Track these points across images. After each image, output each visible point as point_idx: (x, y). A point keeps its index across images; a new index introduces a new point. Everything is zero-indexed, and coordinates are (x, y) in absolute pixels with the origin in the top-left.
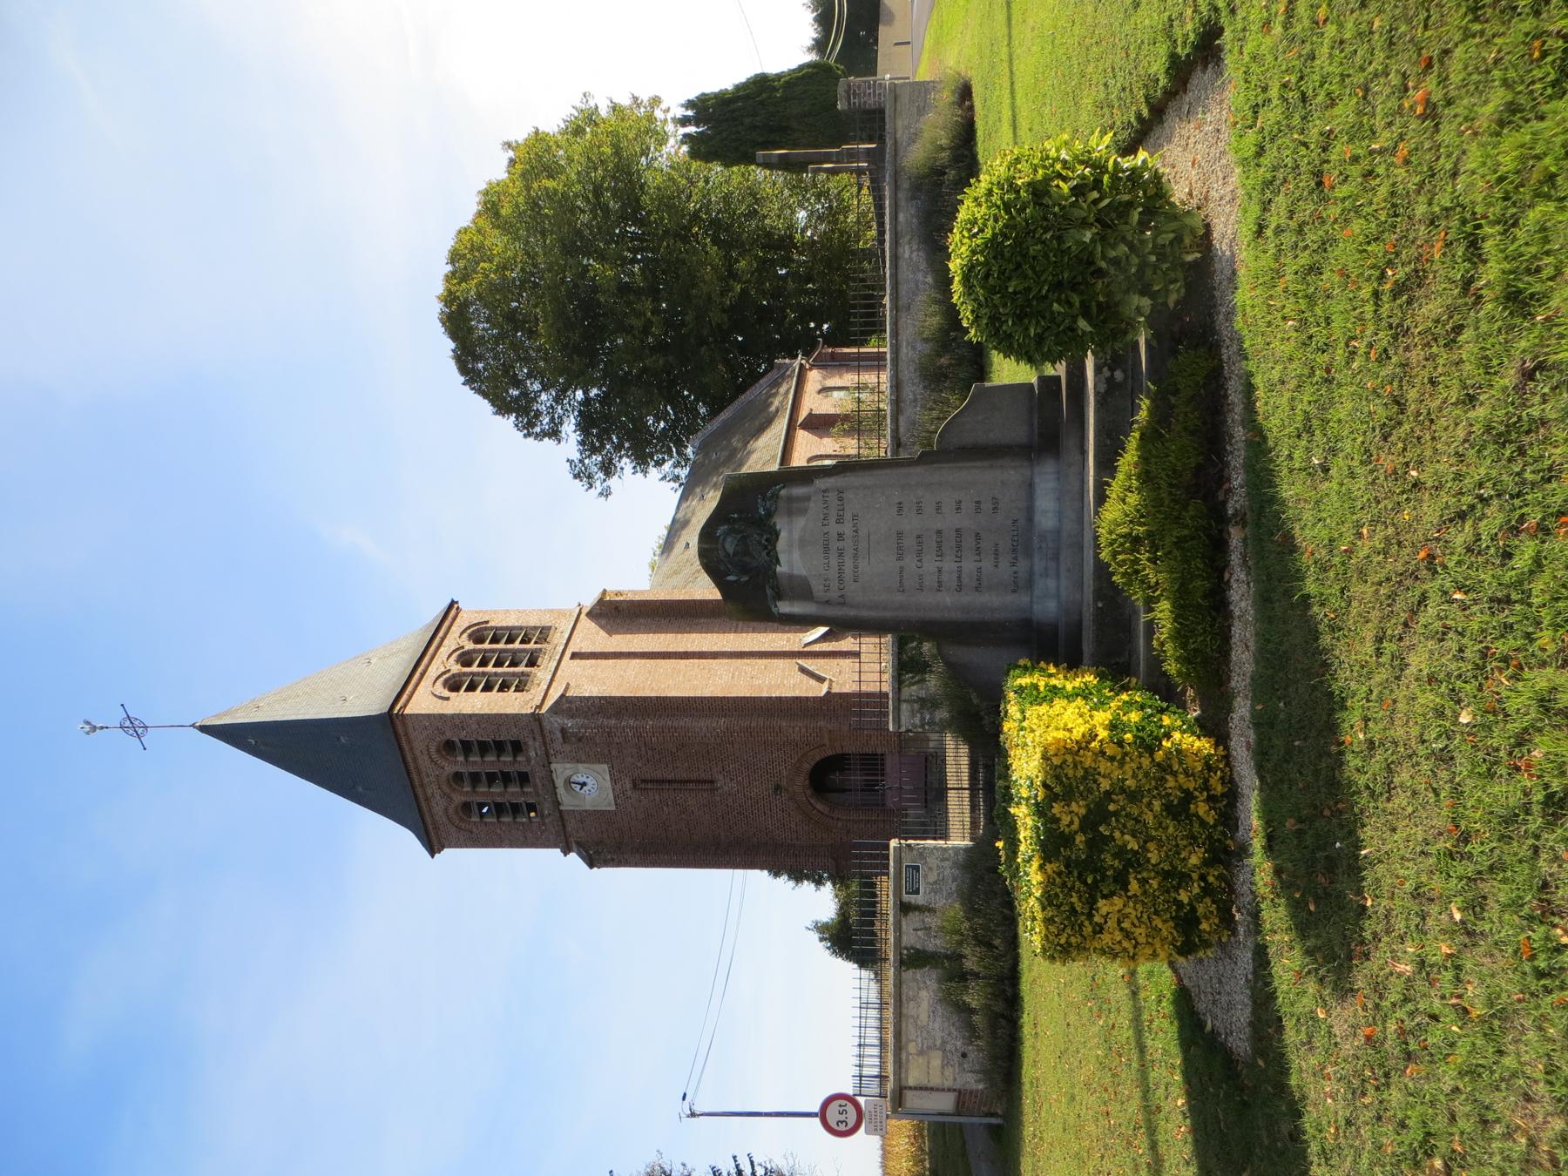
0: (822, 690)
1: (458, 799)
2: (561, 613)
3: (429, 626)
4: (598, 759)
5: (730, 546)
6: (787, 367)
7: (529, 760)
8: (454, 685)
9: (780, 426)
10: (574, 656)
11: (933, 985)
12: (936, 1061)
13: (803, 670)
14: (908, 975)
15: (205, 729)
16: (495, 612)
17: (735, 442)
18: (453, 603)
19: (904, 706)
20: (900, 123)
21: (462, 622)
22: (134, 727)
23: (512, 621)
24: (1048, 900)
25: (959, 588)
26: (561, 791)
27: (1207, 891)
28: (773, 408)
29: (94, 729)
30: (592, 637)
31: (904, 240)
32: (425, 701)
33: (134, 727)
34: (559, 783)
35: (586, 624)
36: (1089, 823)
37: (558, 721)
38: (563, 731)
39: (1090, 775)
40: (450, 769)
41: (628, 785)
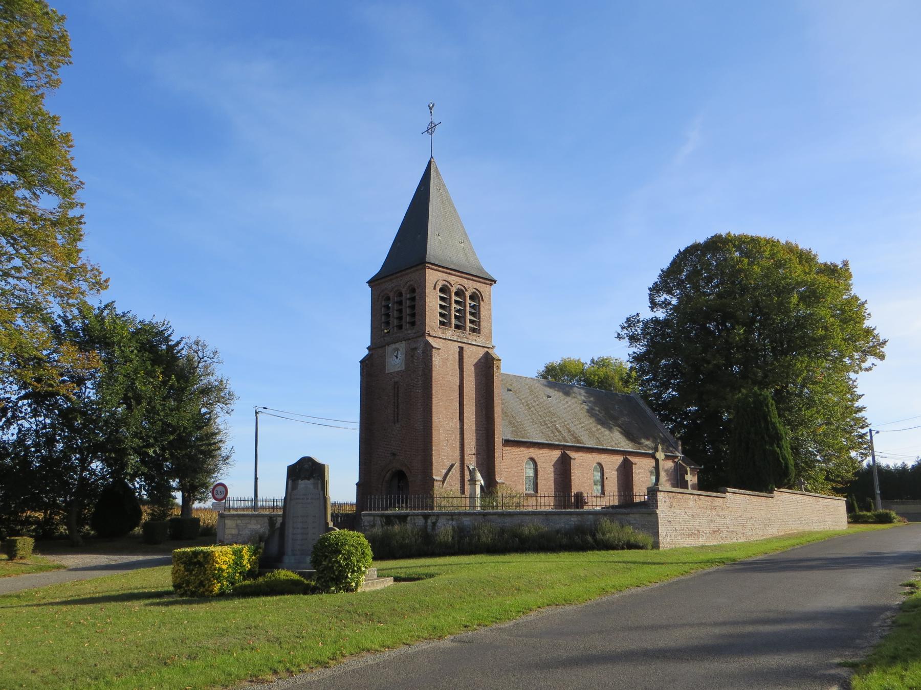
0: (437, 477)
1: (391, 295)
2: (489, 337)
3: (482, 270)
4: (407, 365)
5: (306, 466)
6: (677, 450)
7: (407, 330)
8: (444, 290)
9: (627, 446)
10: (461, 349)
11: (262, 530)
12: (234, 532)
13: (452, 466)
14: (266, 520)
15: (430, 162)
16: (490, 304)
17: (624, 419)
18: (495, 282)
19: (372, 518)
20: (637, 516)
21: (482, 287)
22: (431, 128)
23: (483, 313)
24: (184, 552)
25: (293, 534)
26: (394, 346)
27: (186, 591)
28: (643, 441)
29: (431, 109)
30: (473, 356)
31: (579, 518)
32: (433, 277)
33: (431, 128)
34: (397, 345)
35: (481, 352)
36: (199, 563)
37: (421, 346)
38: (415, 349)
39: (208, 562)
40: (404, 291)
41: (396, 379)
